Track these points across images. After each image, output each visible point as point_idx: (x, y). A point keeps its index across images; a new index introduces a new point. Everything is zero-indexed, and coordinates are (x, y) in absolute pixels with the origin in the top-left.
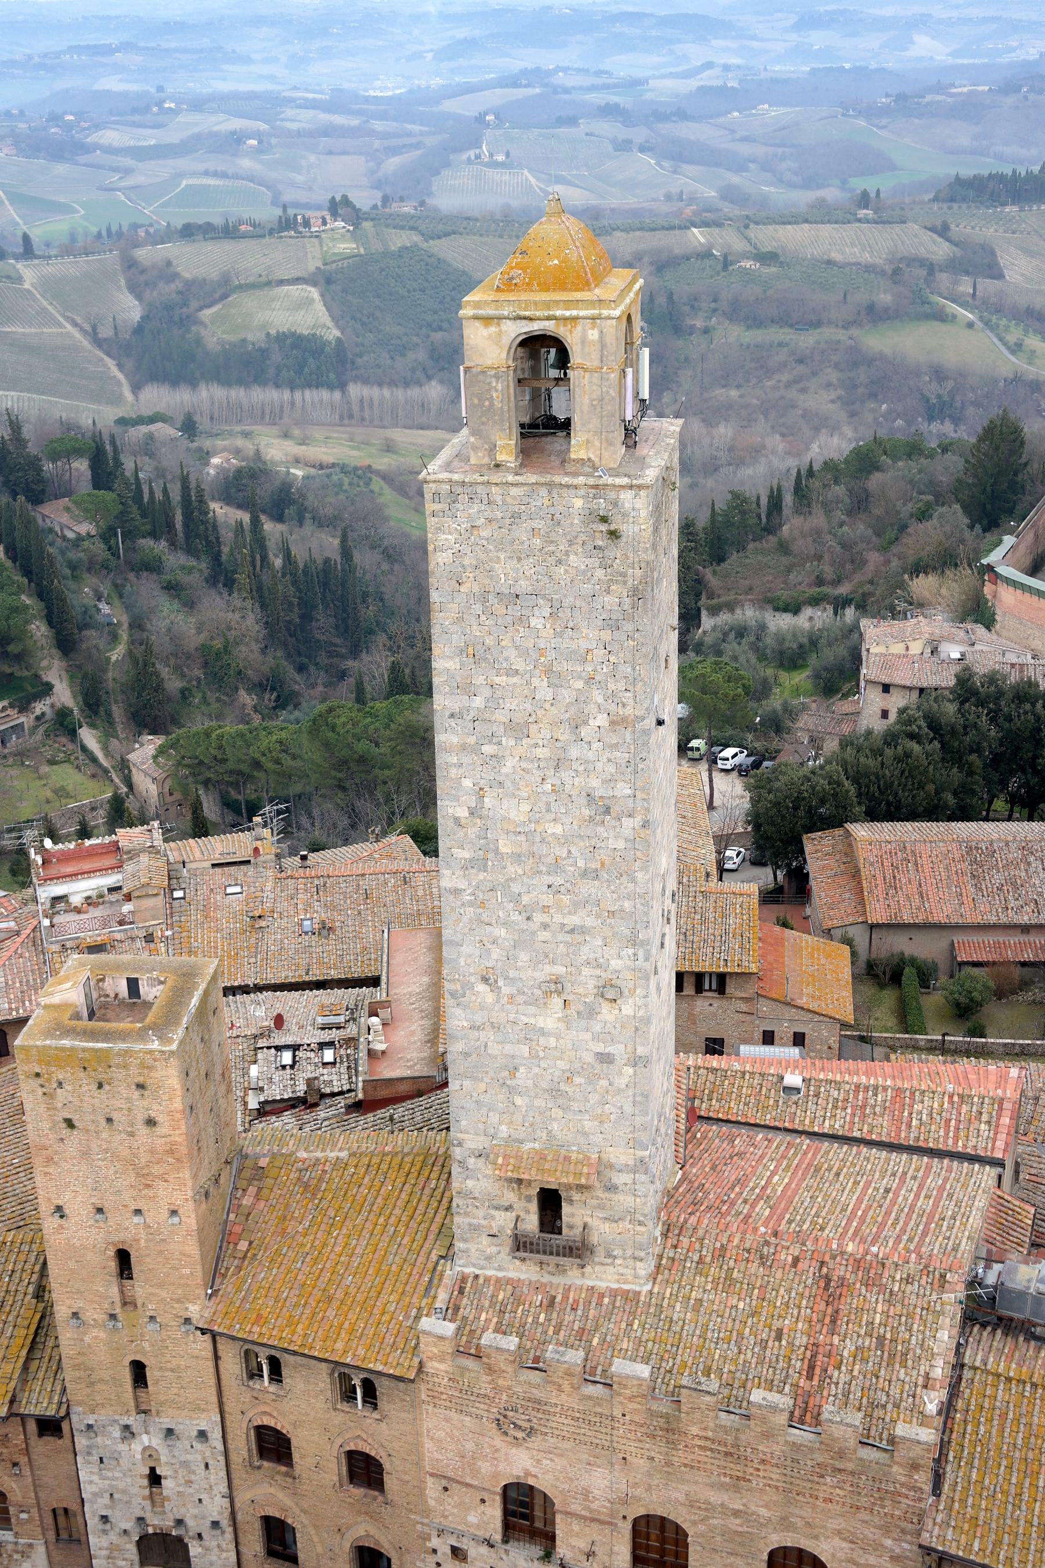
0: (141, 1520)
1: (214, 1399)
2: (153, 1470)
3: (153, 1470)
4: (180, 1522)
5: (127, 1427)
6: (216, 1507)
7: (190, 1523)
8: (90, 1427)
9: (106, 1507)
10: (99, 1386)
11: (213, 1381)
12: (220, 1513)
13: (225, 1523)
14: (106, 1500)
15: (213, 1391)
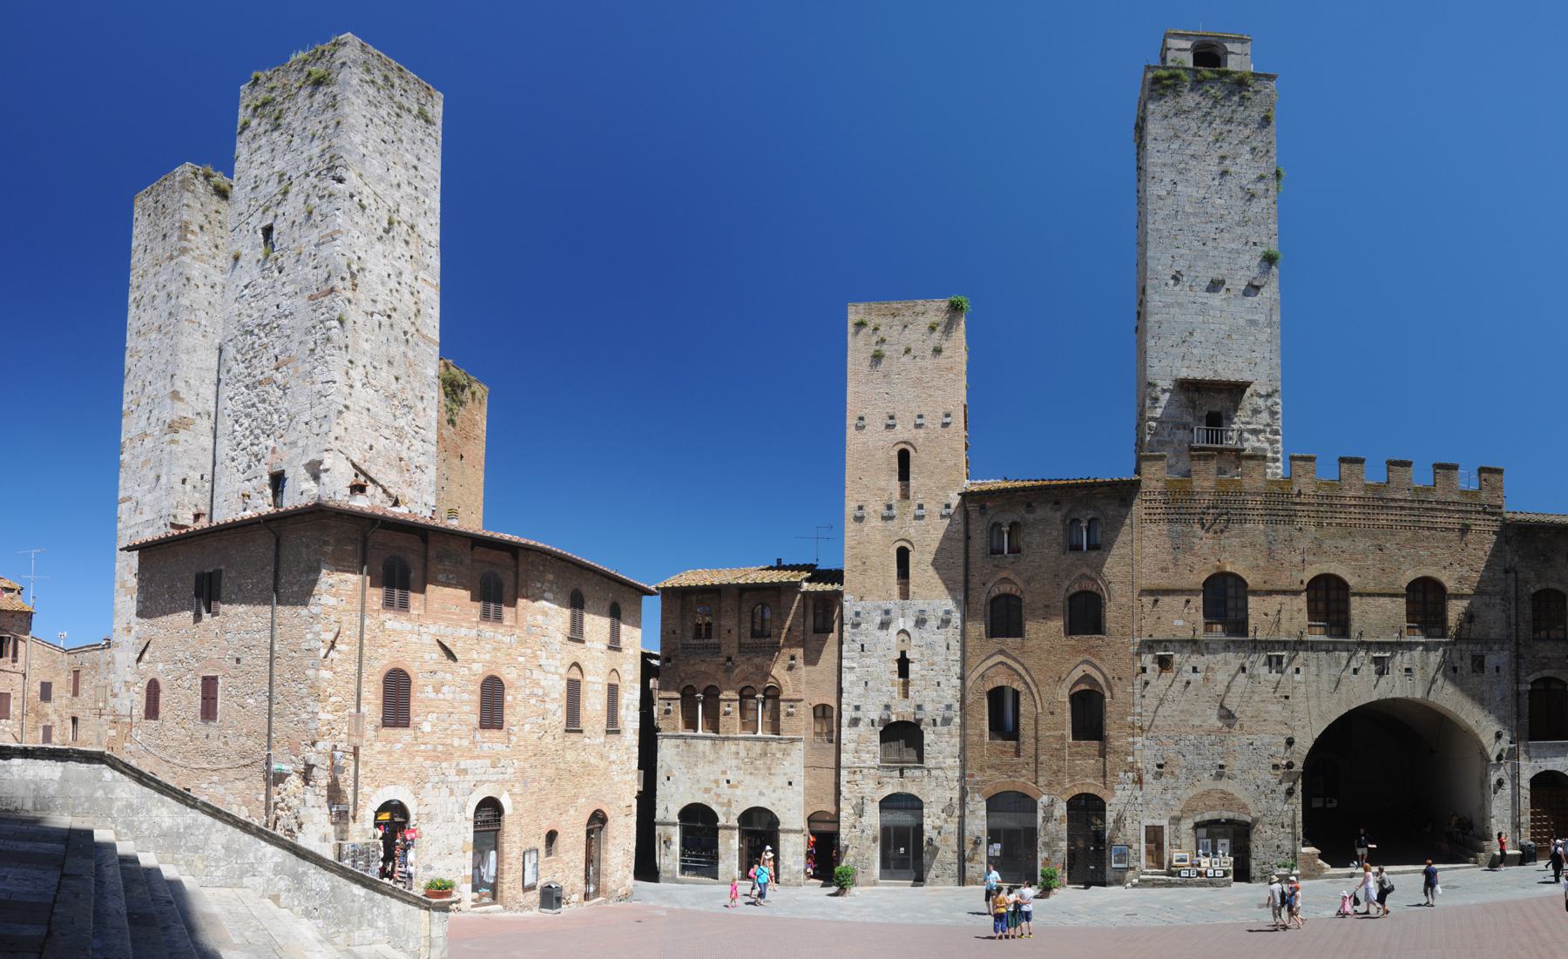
0: (887, 707)
1: (961, 578)
2: (903, 653)
3: (903, 653)
4: (919, 707)
5: (887, 612)
6: (950, 693)
7: (928, 707)
8: (857, 614)
9: (860, 696)
10: (871, 573)
11: (961, 561)
12: (954, 697)
13: (957, 706)
14: (860, 689)
15: (961, 571)
